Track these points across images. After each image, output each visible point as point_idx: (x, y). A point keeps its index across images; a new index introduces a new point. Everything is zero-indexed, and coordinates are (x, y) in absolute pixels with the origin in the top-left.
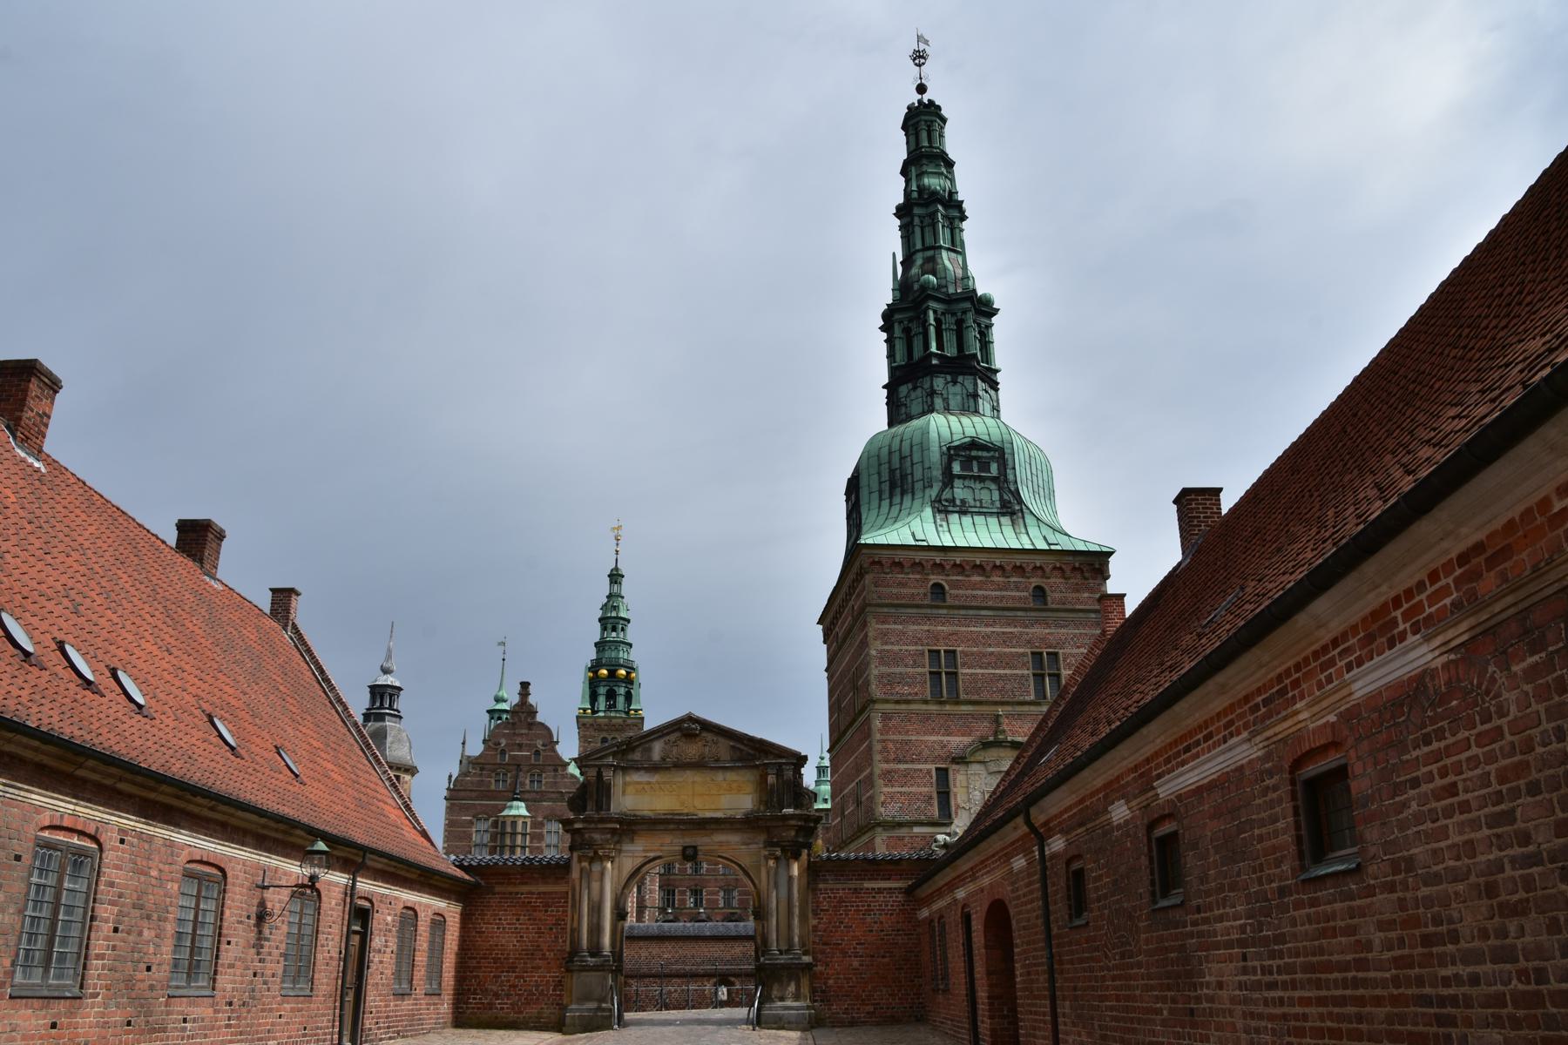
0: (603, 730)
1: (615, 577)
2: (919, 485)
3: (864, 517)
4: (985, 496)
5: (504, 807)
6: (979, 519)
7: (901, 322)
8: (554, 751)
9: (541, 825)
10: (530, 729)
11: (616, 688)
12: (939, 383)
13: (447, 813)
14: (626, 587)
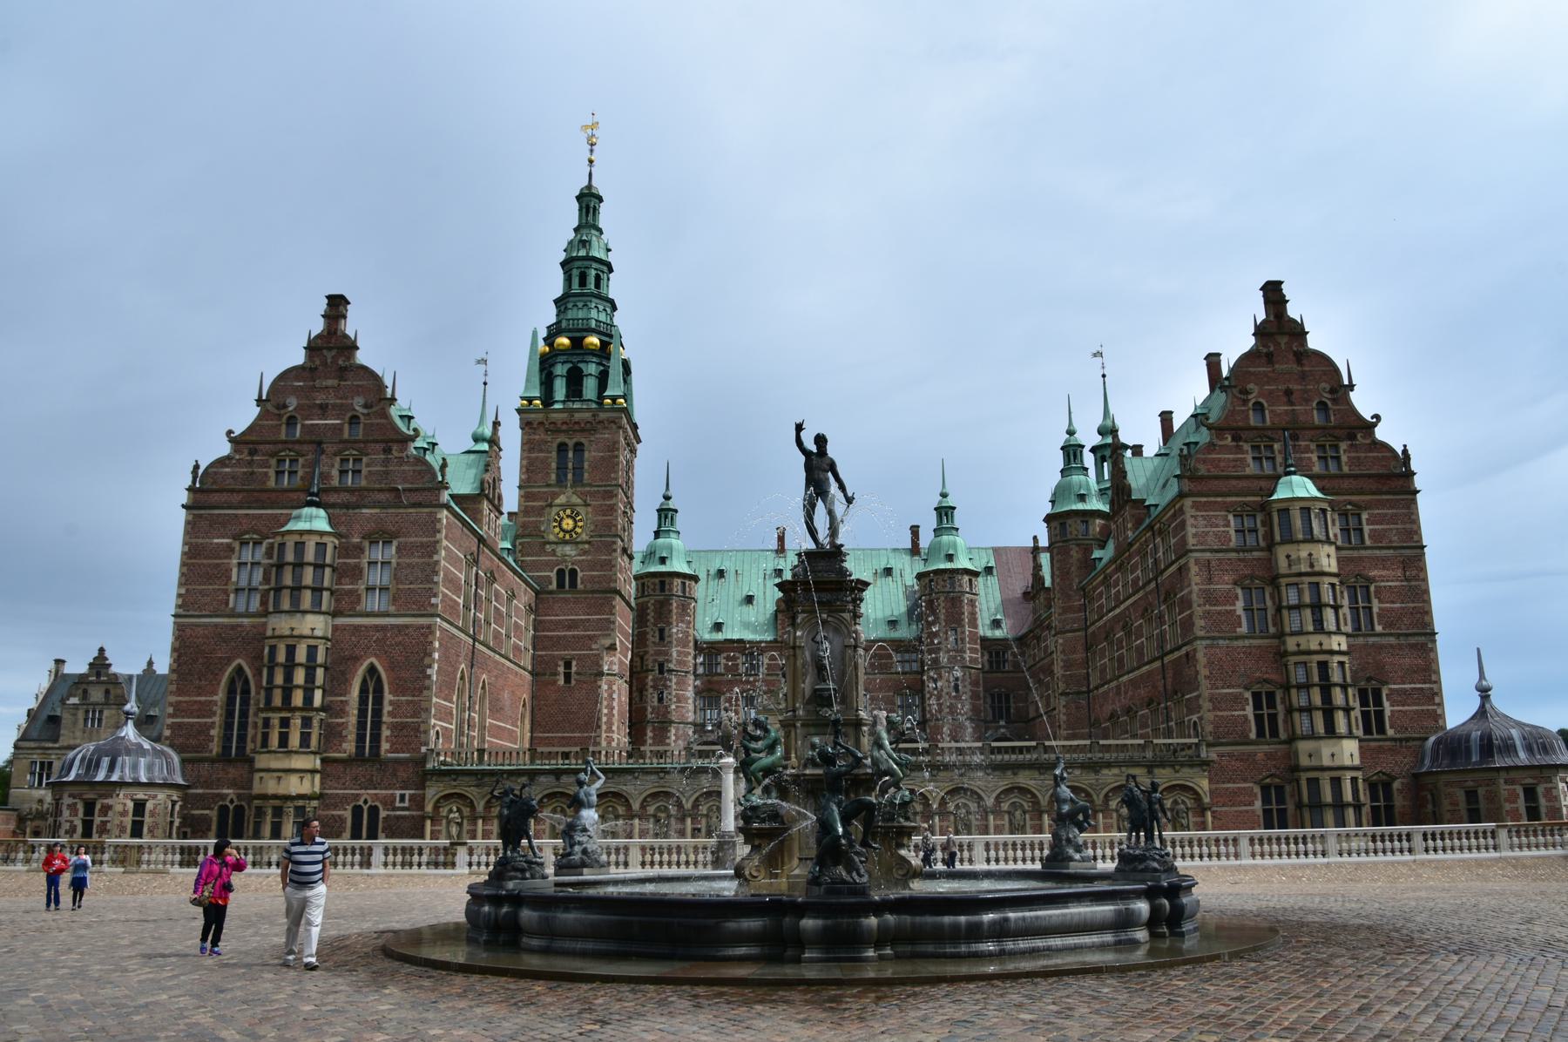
0: (559, 431)
1: (589, 201)
5: (288, 519)
8: (385, 415)
9: (359, 550)
10: (341, 378)
11: (581, 365)
13: (186, 533)
14: (606, 216)
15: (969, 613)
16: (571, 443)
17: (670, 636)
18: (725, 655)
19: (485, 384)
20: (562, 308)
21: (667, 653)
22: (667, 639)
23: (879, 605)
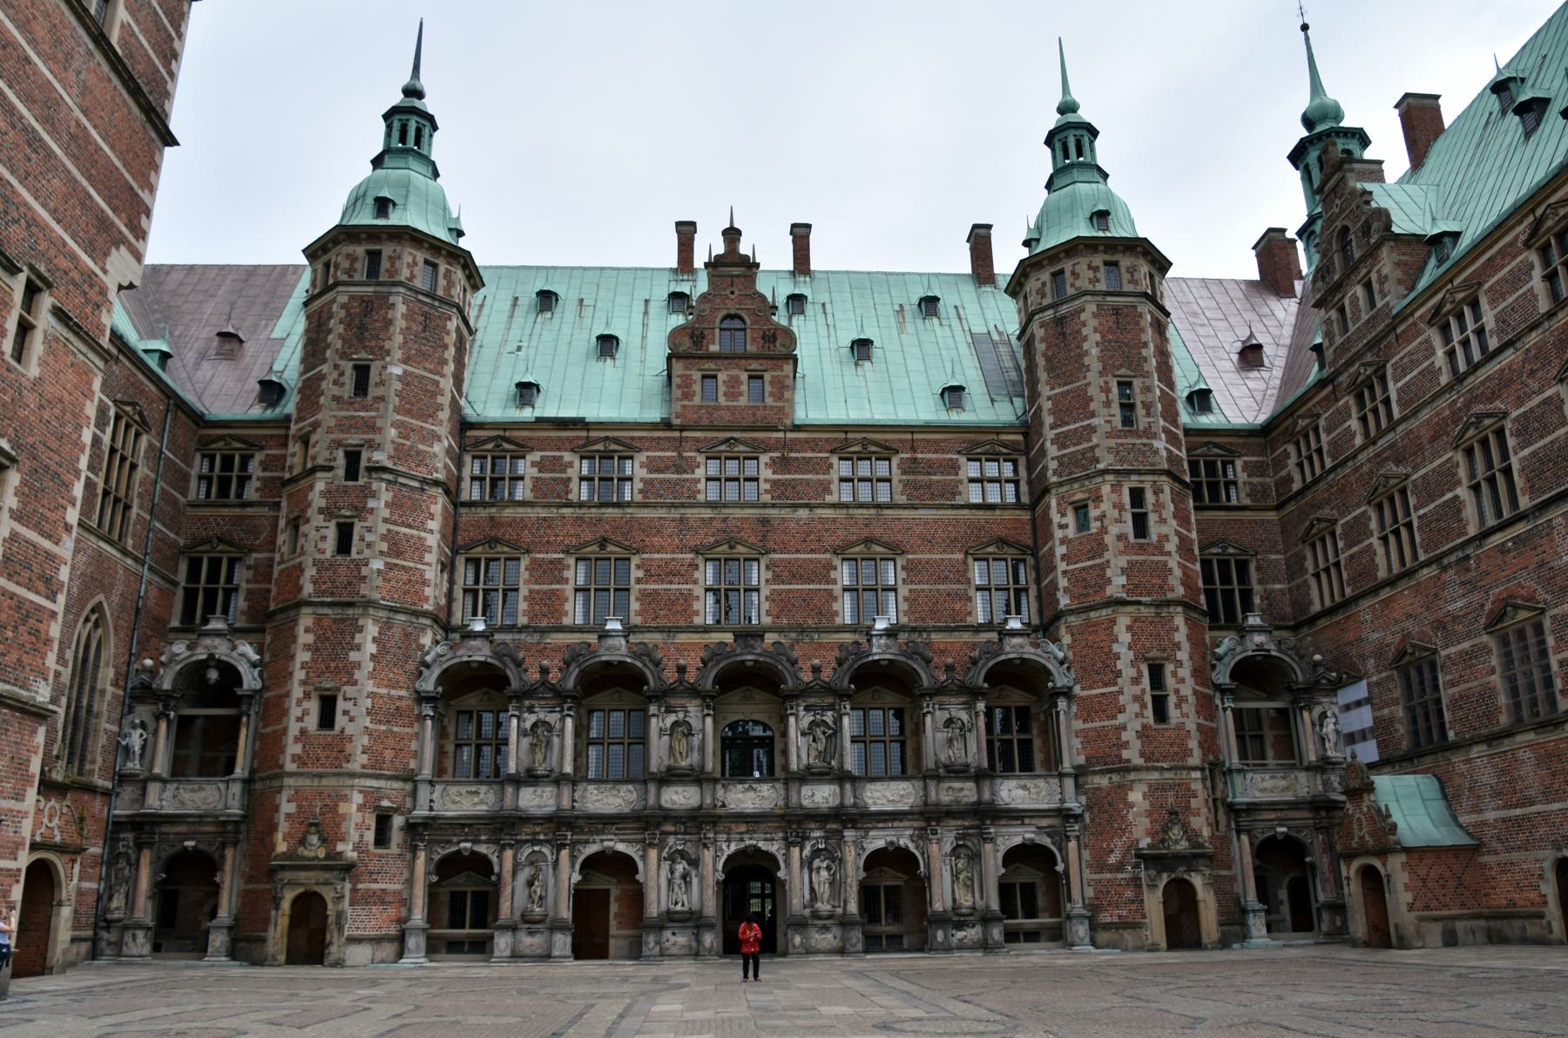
15: (1156, 347)
17: (382, 383)
18: (536, 456)
21: (371, 427)
22: (373, 391)
23: (915, 364)
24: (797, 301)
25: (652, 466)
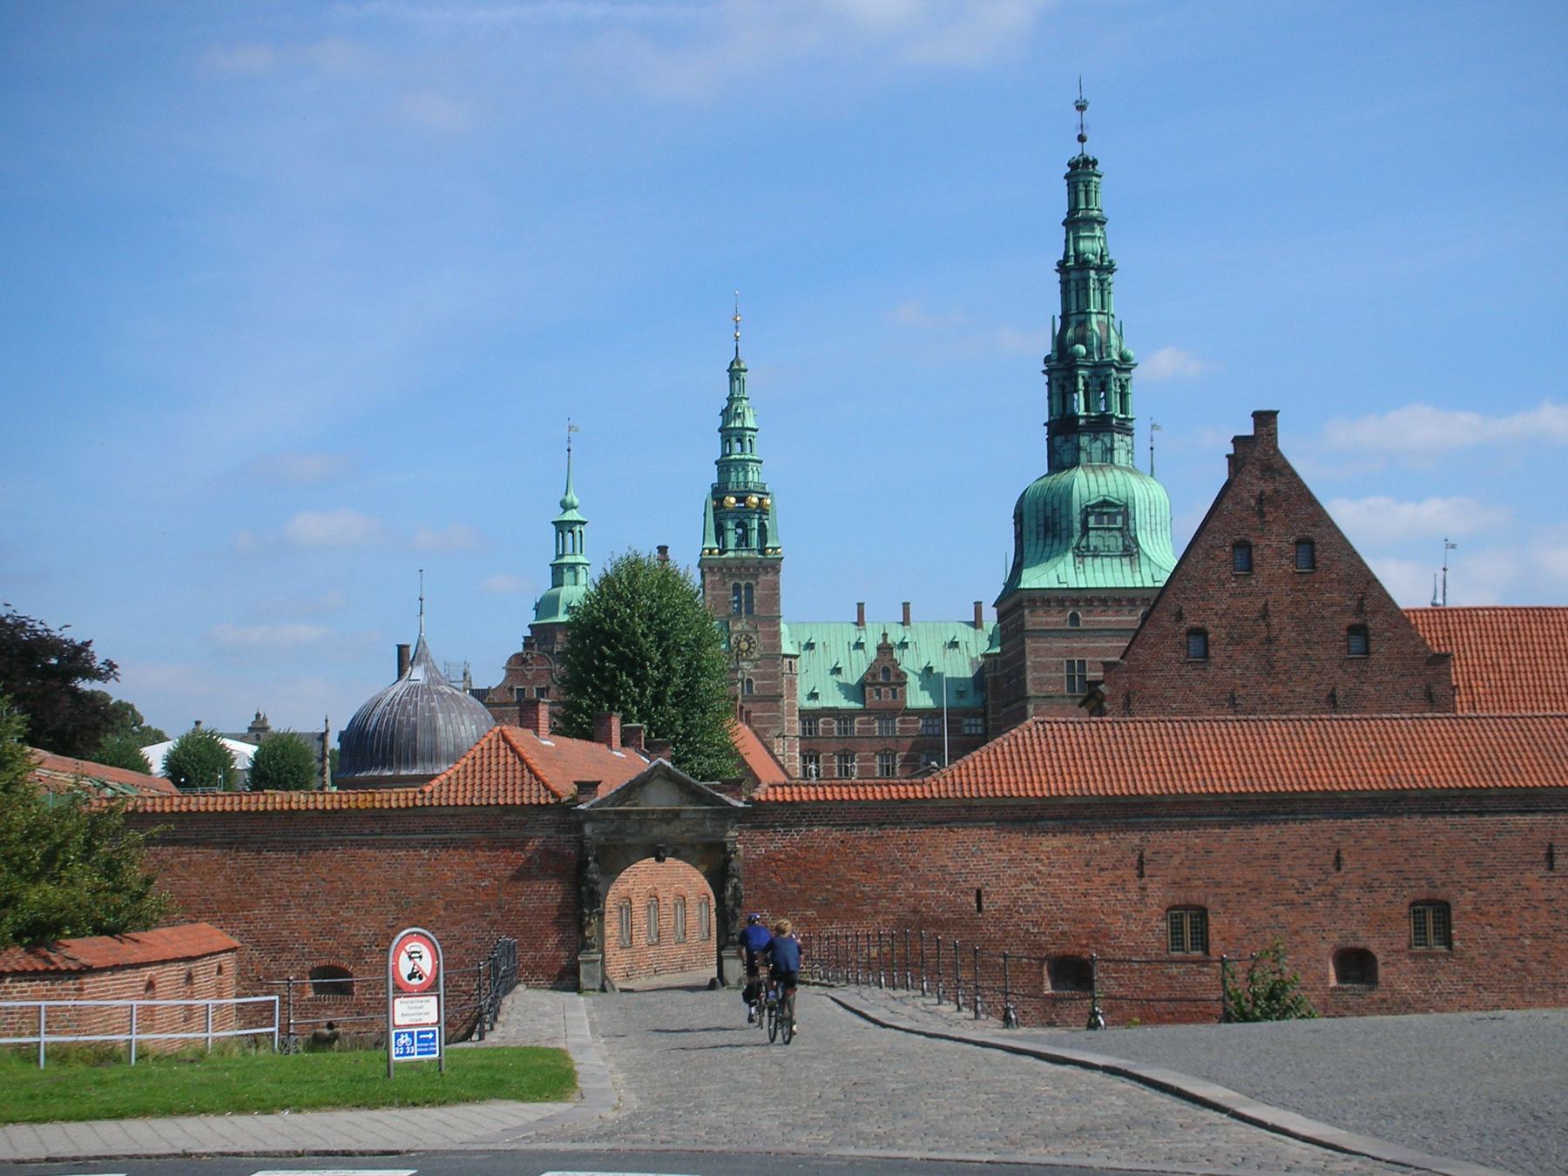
2: (1064, 533)
3: (1025, 551)
4: (1111, 542)
6: (1107, 561)
7: (1057, 380)
11: (745, 520)
12: (1084, 440)
16: (743, 583)
18: (821, 720)
19: (569, 450)
20: (725, 468)
24: (904, 645)
25: (860, 723)
